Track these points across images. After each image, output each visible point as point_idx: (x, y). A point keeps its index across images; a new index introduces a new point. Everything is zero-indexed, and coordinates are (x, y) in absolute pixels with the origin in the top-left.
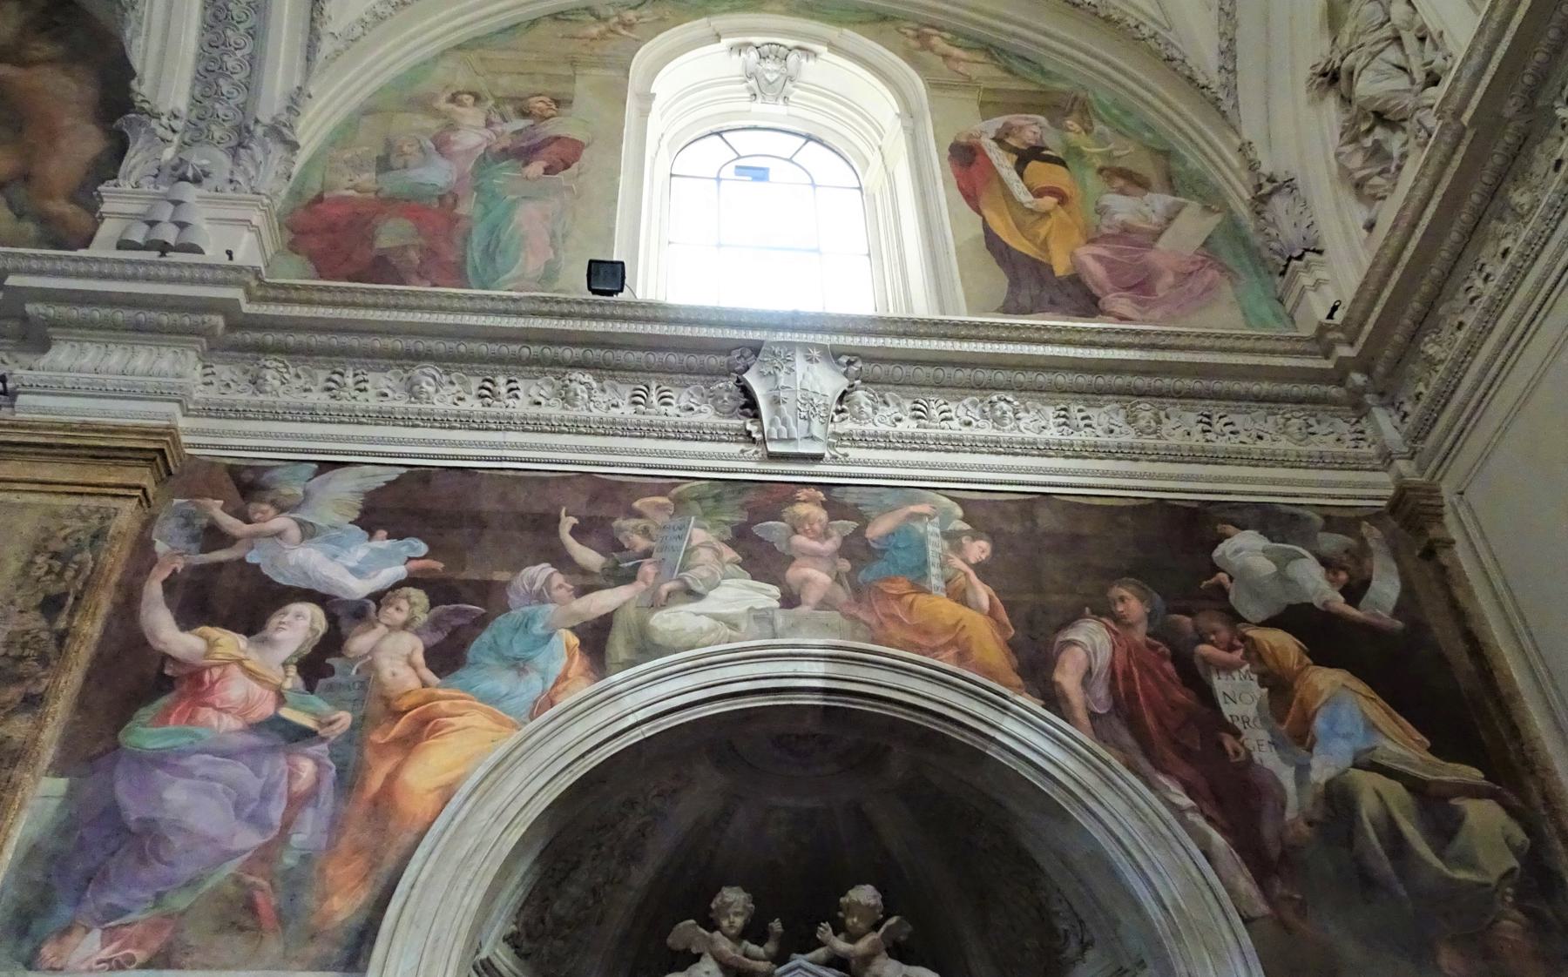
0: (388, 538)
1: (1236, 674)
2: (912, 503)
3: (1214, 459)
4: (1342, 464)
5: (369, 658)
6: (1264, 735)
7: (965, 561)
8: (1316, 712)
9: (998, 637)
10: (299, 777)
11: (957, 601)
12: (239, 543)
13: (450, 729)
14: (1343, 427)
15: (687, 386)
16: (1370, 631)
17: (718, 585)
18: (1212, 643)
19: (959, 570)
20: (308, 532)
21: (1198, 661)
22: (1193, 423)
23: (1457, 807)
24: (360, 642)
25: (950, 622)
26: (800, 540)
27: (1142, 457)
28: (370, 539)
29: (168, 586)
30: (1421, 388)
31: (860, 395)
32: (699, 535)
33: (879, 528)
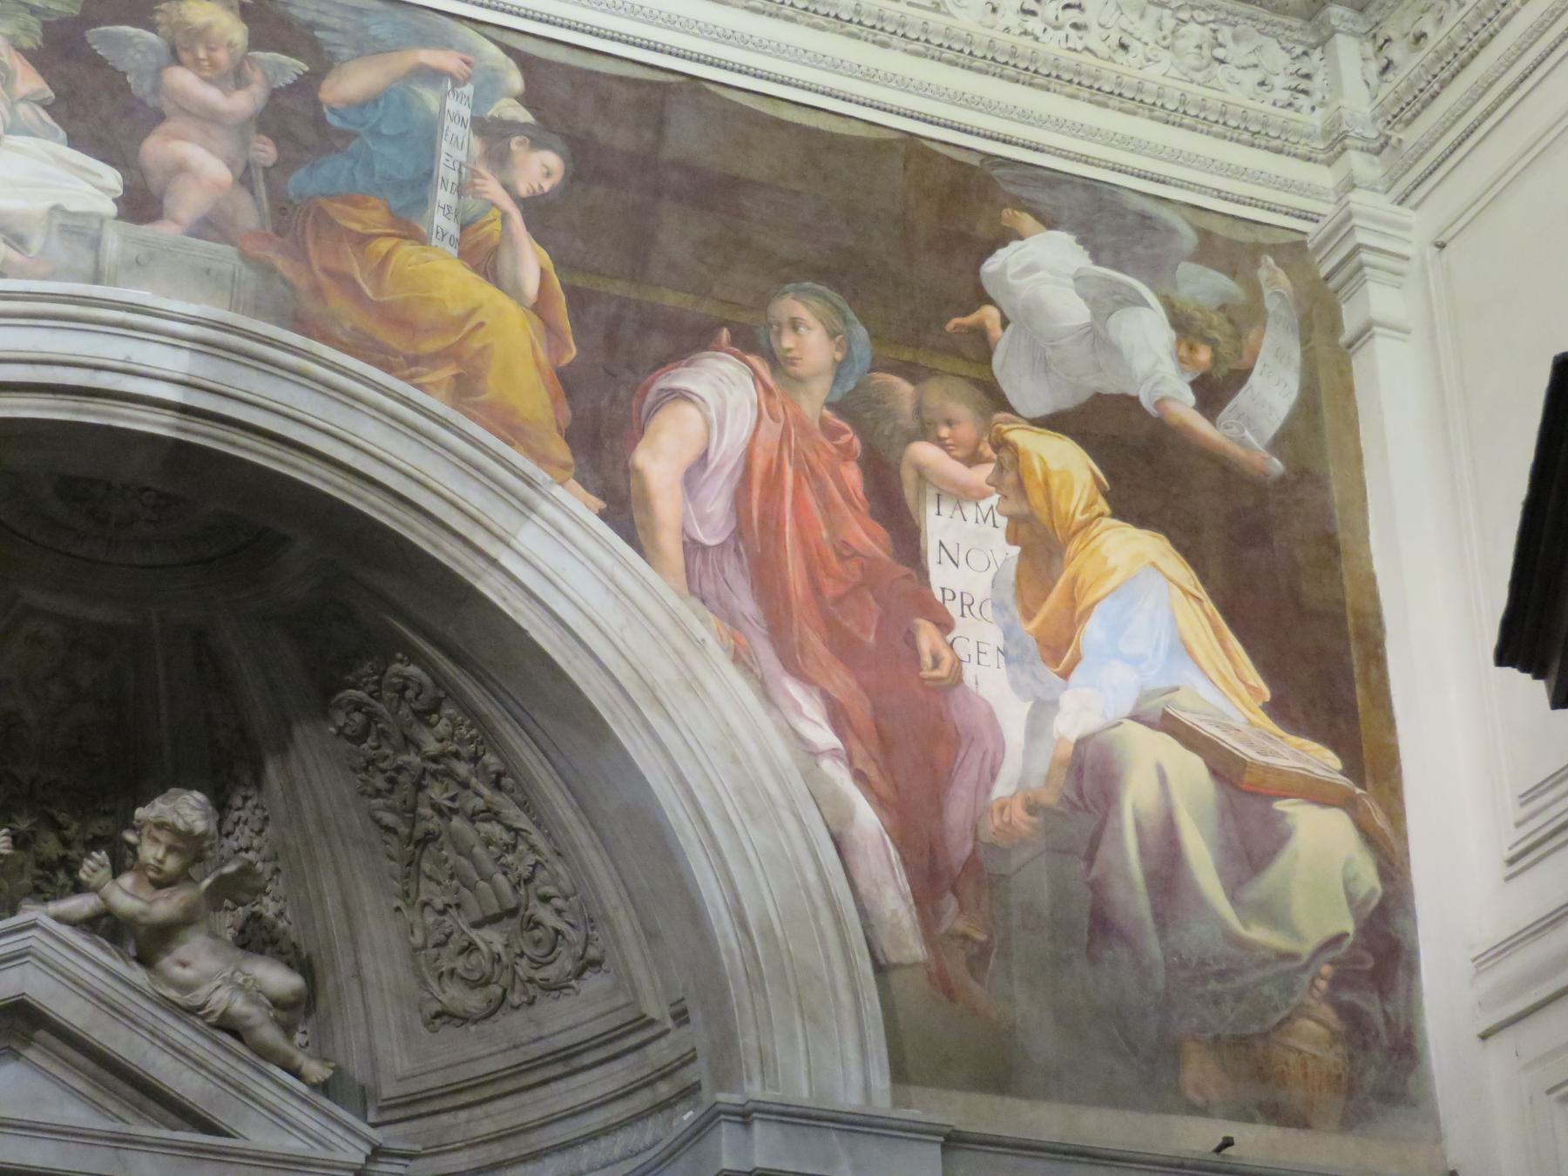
1: (970, 510)
3: (1030, 74)
4: (1255, 135)
6: (993, 637)
7: (508, 188)
8: (1090, 609)
9: (543, 356)
11: (475, 268)
14: (1276, 58)
16: (1225, 470)
18: (940, 443)
19: (493, 204)
21: (908, 475)
23: (1283, 815)
25: (456, 309)
26: (182, 79)
27: (895, 40)
30: (1427, 25)
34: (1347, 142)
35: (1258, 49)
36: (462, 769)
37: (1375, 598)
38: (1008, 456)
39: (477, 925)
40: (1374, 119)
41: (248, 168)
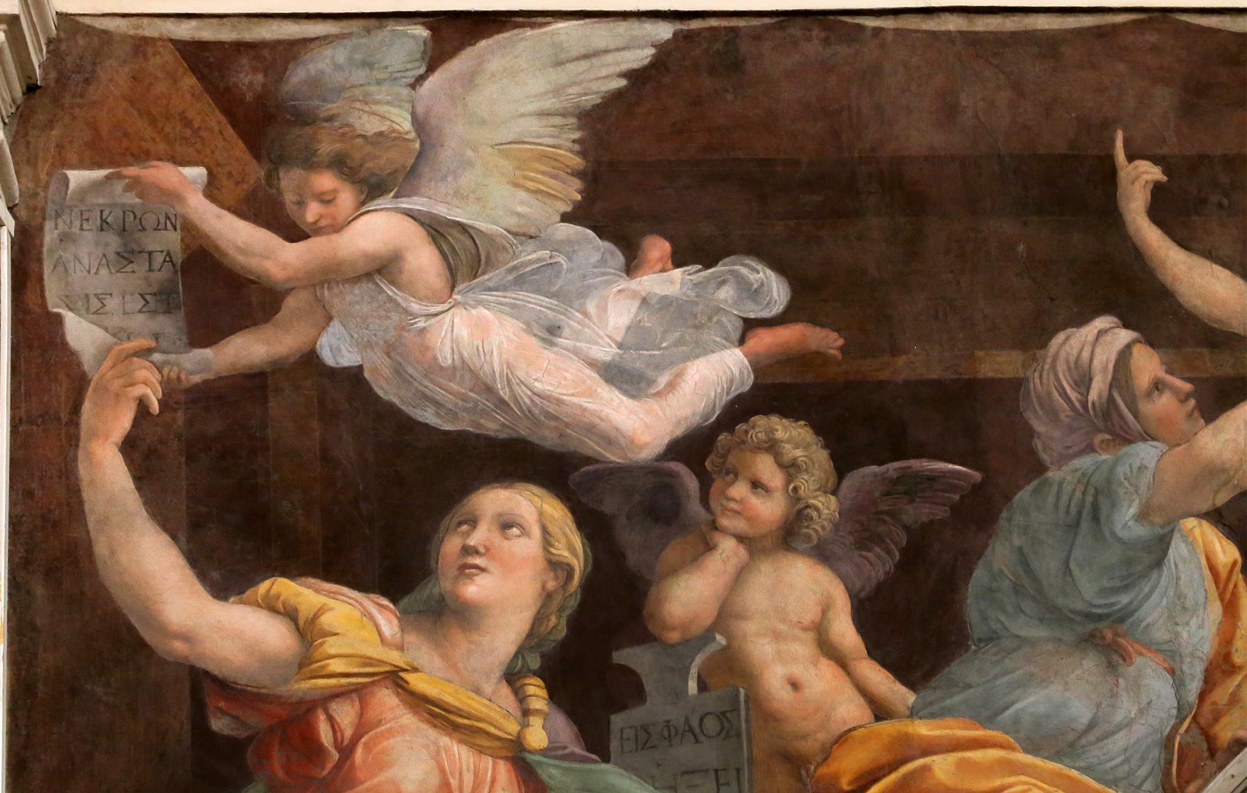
0: (679, 260)
5: (721, 640)
12: (290, 303)
28: (632, 266)
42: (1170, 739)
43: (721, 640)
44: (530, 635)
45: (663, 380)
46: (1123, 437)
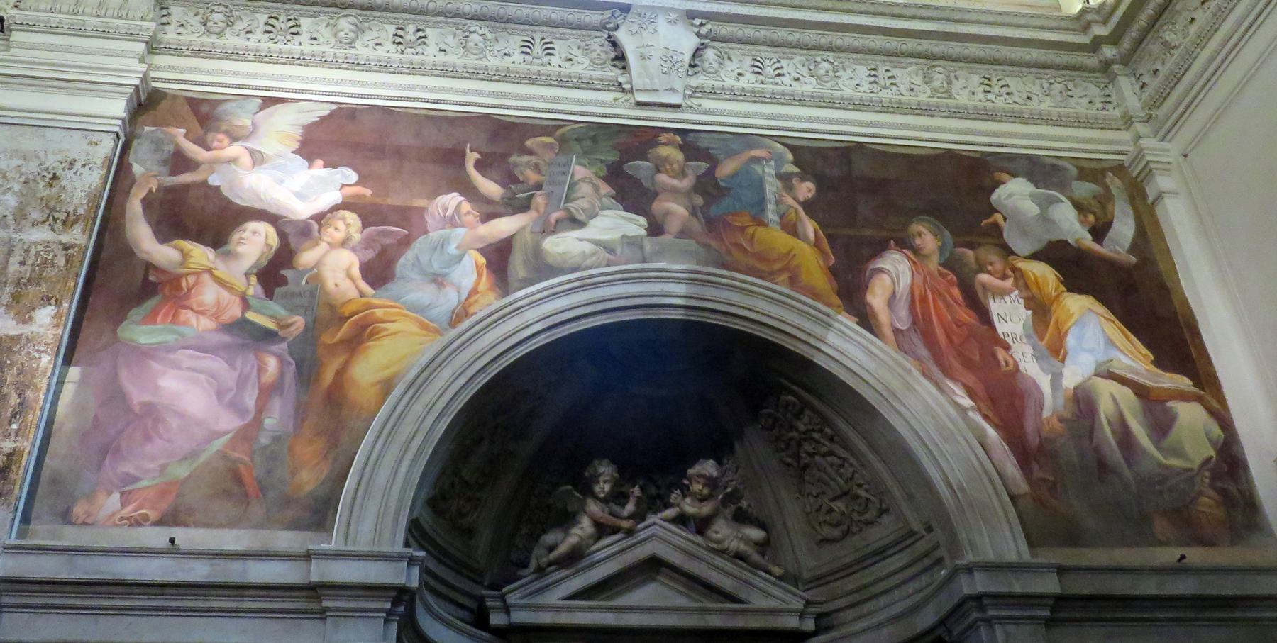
0: (325, 167)
2: (752, 149)
7: (795, 199)
9: (821, 263)
10: (266, 371)
11: (789, 233)
13: (385, 333)
14: (1093, 91)
15: (567, 39)
17: (597, 215)
19: (790, 207)
20: (258, 159)
22: (976, 84)
24: (307, 257)
25: (785, 251)
26: (663, 178)
27: (936, 113)
28: (310, 167)
29: (147, 203)
30: (1158, 66)
31: (710, 54)
32: (580, 171)
33: (727, 168)
34: (1133, 119)
35: (1085, 89)
36: (816, 436)
37: (1189, 308)
38: (1019, 275)
39: (832, 500)
40: (1143, 108)
41: (694, 208)
42: (455, 309)
43: (315, 270)
44: (256, 263)
45: (314, 197)
46: (454, 225)
